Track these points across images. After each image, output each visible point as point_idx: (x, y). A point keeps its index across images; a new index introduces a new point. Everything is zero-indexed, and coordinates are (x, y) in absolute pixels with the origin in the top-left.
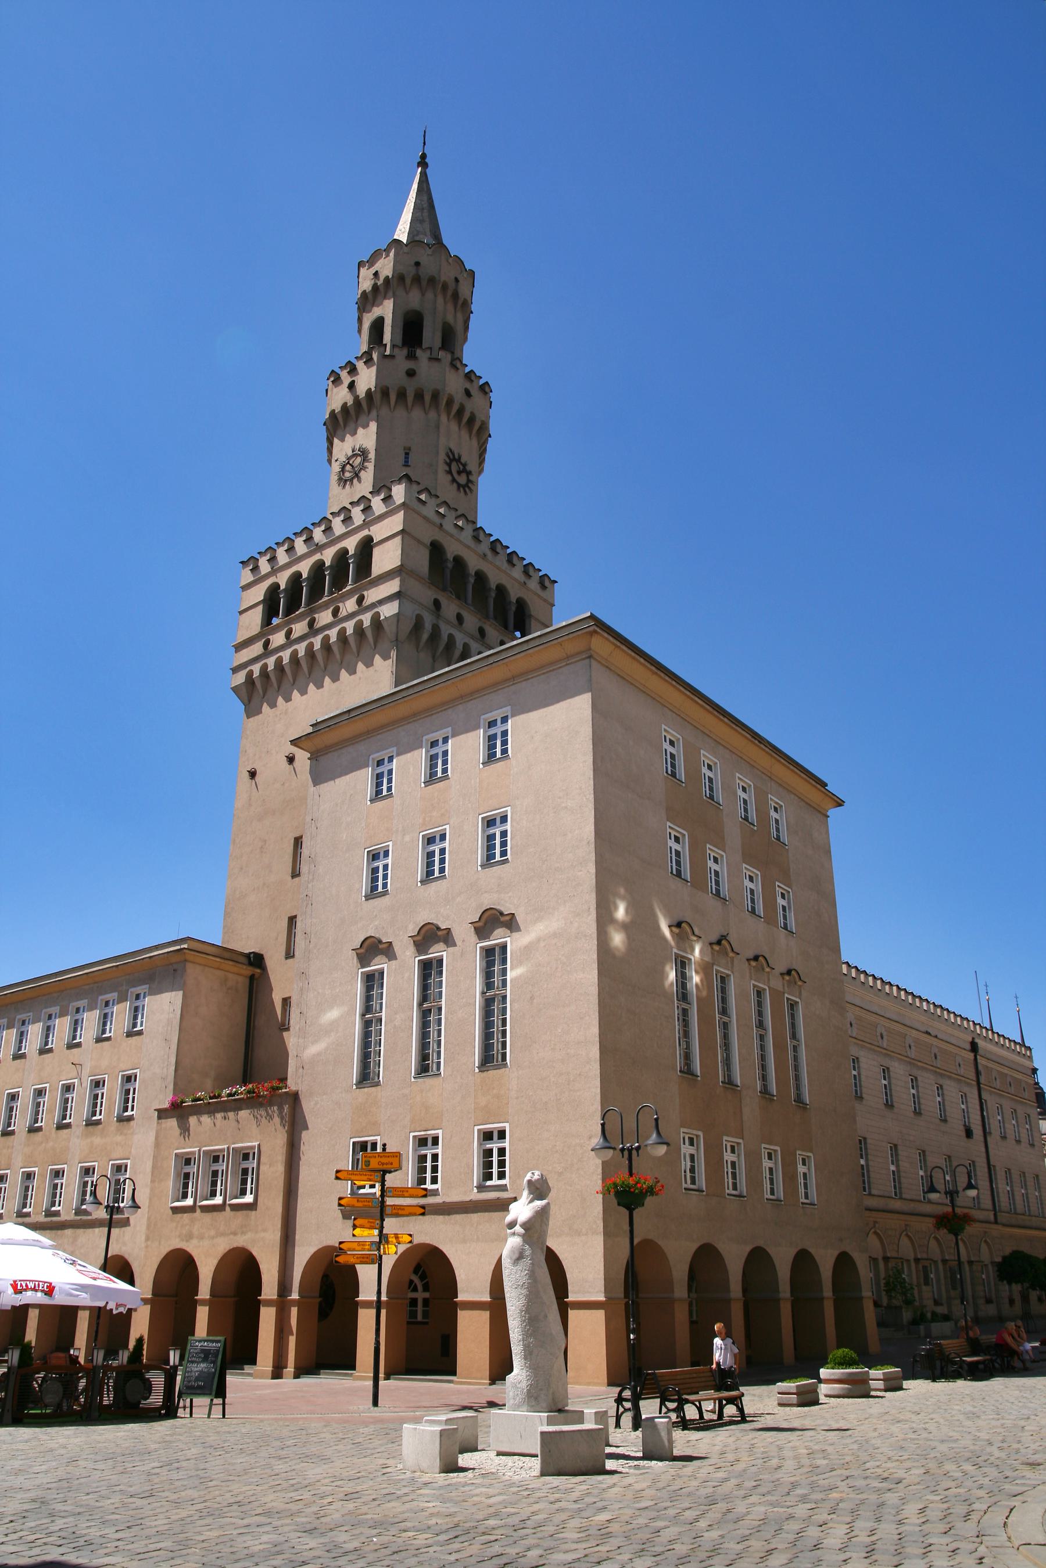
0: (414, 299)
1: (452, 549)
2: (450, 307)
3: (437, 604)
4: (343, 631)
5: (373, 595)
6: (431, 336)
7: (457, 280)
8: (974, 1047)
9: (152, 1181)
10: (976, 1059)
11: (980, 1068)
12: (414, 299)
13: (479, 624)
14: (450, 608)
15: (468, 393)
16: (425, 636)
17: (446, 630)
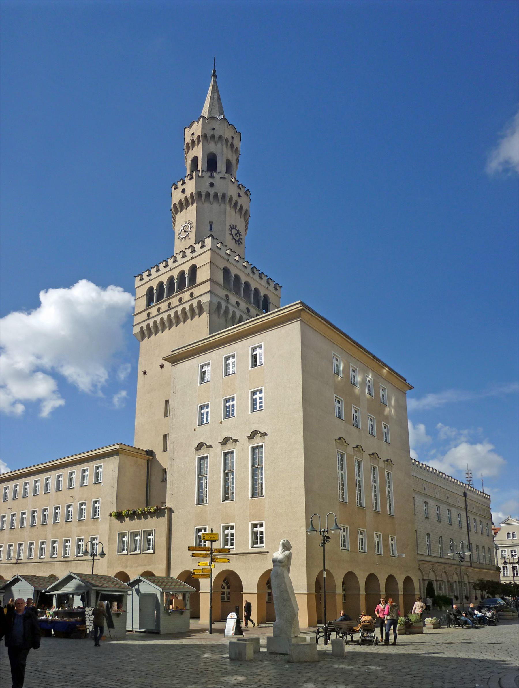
0: (213, 148)
1: (234, 271)
2: (230, 151)
3: (227, 296)
4: (184, 309)
5: (197, 291)
6: (221, 166)
7: (232, 138)
8: (465, 495)
9: (109, 544)
10: (465, 500)
11: (467, 503)
12: (213, 148)
13: (247, 306)
14: (233, 299)
15: (239, 196)
16: (222, 312)
17: (231, 309)
